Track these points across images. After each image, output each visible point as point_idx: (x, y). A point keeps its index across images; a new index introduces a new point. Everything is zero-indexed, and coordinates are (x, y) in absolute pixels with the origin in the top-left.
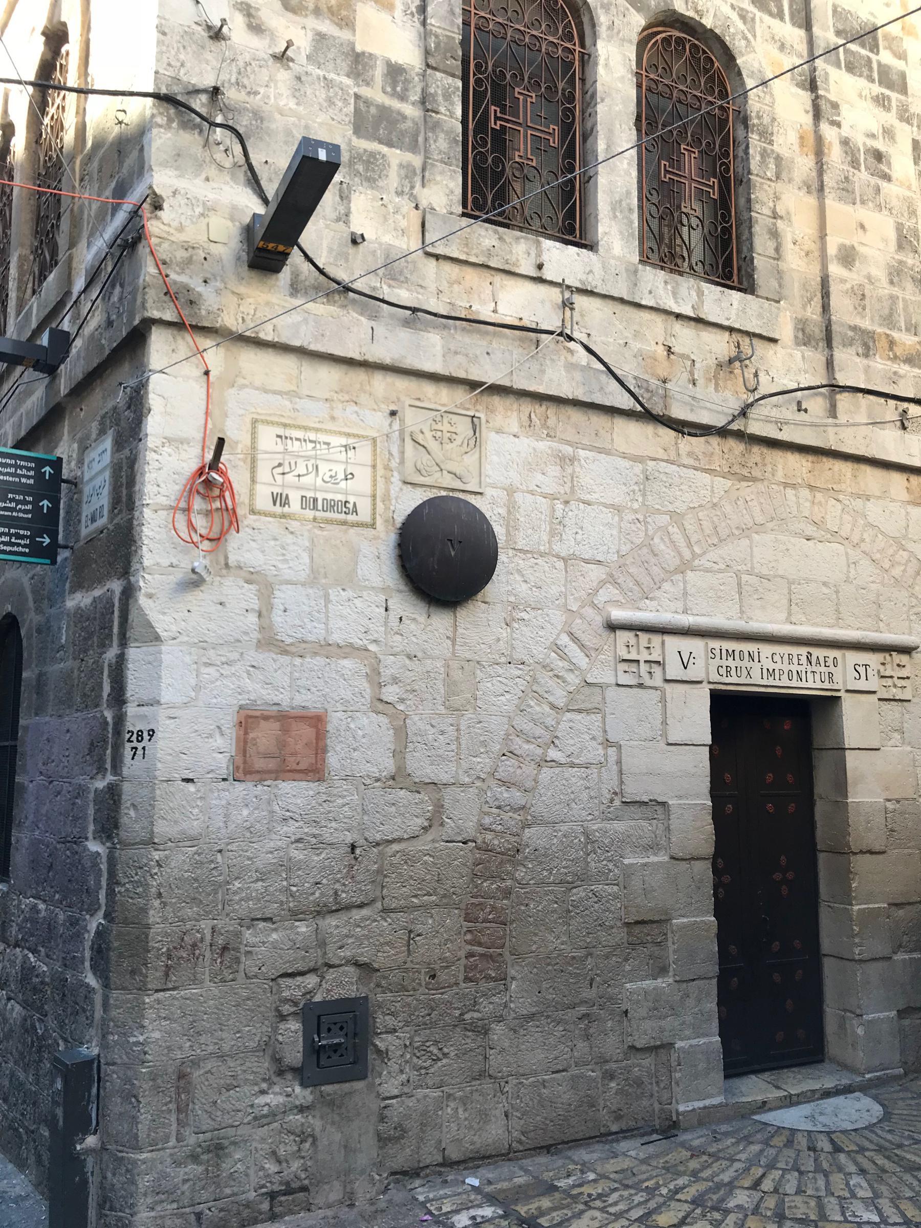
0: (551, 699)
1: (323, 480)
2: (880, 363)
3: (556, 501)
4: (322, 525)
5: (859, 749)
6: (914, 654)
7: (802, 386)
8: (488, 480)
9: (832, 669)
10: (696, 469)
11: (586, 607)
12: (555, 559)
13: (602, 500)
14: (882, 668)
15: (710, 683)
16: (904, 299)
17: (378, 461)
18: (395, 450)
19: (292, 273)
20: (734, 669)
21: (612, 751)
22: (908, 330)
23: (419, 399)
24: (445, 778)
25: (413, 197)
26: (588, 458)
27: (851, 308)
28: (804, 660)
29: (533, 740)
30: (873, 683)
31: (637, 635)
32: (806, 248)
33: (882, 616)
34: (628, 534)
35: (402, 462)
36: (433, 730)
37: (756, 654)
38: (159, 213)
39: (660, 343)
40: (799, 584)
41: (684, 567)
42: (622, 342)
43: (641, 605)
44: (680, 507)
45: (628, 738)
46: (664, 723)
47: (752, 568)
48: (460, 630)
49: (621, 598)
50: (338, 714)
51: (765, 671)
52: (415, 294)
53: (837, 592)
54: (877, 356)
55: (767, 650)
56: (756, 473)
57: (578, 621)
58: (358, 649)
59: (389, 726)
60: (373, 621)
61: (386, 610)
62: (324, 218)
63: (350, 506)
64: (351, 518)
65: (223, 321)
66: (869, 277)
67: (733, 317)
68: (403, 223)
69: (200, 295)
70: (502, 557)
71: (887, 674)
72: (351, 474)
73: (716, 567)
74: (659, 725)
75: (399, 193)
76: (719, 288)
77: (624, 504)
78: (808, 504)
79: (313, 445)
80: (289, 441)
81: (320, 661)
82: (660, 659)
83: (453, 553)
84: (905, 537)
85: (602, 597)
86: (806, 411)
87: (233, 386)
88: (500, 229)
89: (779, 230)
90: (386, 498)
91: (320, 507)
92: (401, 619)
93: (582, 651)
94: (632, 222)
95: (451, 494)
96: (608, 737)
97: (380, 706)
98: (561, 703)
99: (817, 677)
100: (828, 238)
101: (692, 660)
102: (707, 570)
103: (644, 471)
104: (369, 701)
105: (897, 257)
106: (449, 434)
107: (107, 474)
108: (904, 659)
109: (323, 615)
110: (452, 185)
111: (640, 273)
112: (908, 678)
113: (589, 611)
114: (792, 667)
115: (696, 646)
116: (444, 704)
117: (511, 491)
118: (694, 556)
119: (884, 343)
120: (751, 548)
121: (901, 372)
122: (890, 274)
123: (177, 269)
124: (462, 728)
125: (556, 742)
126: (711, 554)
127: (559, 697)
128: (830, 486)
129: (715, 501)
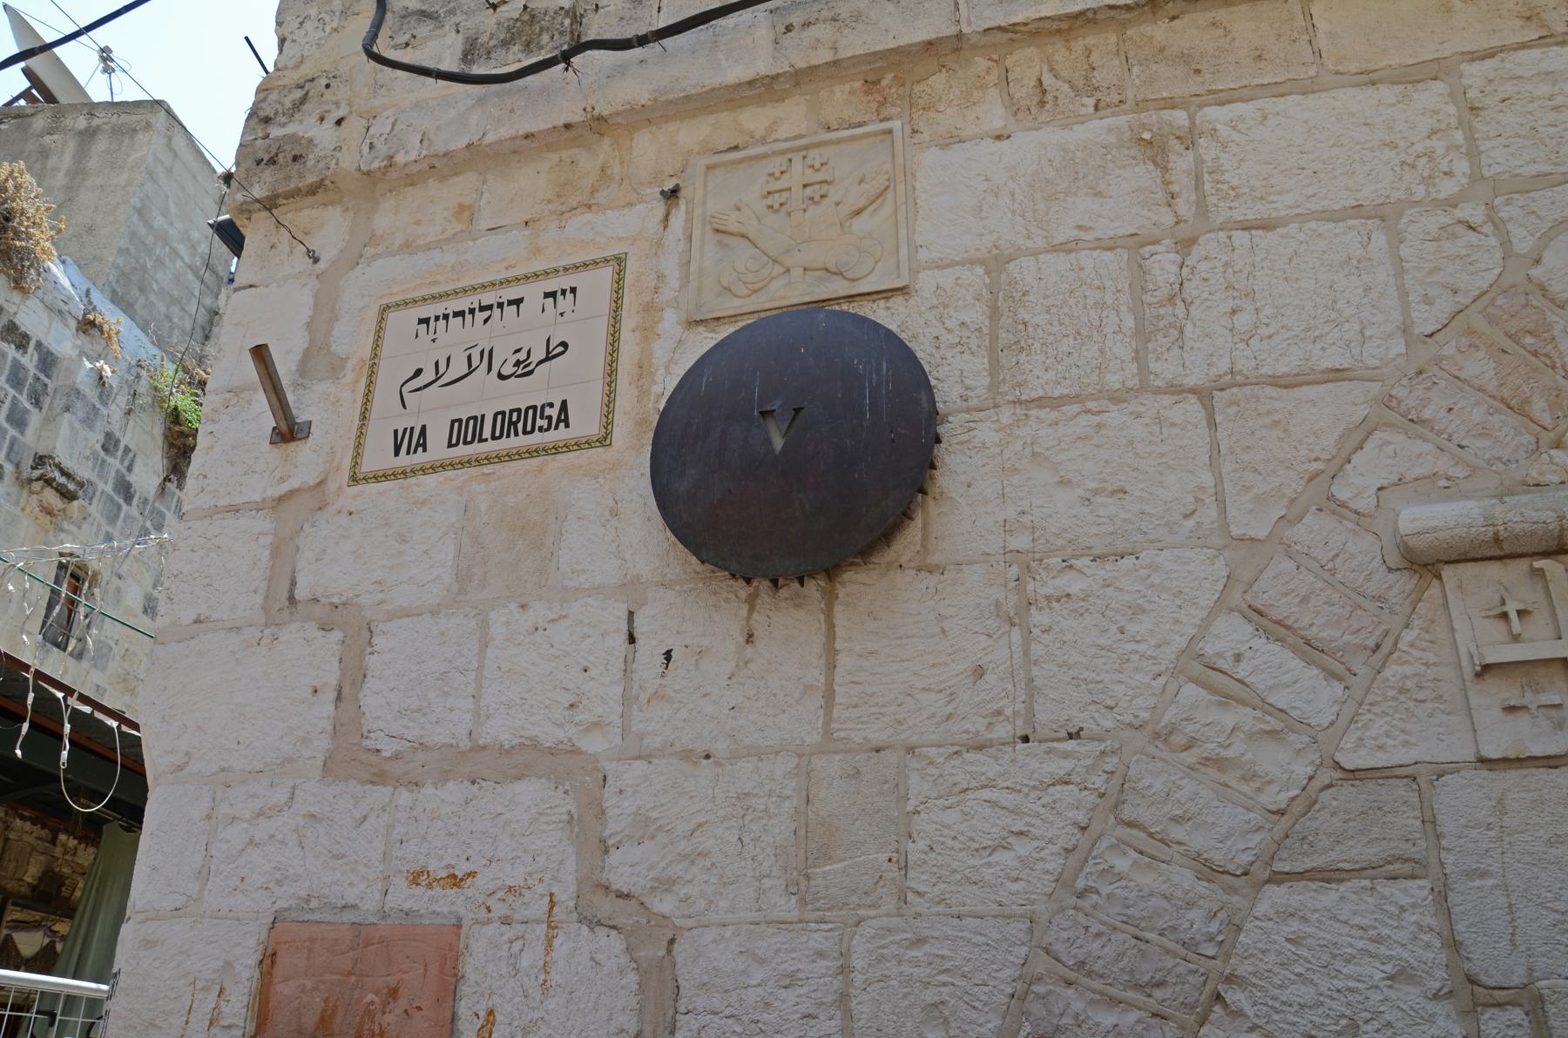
0: (1199, 841)
1: (501, 377)
3: (1148, 249)
4: (486, 470)
8: (923, 255)
12: (1166, 400)
13: (1313, 205)
18: (670, 266)
23: (736, 148)
26: (1241, 119)
29: (1130, 994)
34: (1431, 272)
36: (758, 975)
48: (844, 661)
49: (1443, 465)
50: (490, 930)
58: (551, 752)
59: (625, 959)
60: (593, 672)
61: (632, 639)
64: (560, 435)
65: (337, 164)
72: (564, 345)
77: (1397, 195)
79: (487, 313)
80: (442, 323)
81: (454, 791)
83: (778, 443)
87: (358, 264)
90: (643, 371)
91: (487, 433)
92: (668, 655)
93: (1310, 662)
96: (1474, 968)
97: (605, 907)
98: (1240, 851)
104: (572, 889)
106: (809, 191)
109: (471, 676)
116: (791, 889)
117: (996, 262)
123: (284, 119)
124: (858, 963)
125: (1234, 996)
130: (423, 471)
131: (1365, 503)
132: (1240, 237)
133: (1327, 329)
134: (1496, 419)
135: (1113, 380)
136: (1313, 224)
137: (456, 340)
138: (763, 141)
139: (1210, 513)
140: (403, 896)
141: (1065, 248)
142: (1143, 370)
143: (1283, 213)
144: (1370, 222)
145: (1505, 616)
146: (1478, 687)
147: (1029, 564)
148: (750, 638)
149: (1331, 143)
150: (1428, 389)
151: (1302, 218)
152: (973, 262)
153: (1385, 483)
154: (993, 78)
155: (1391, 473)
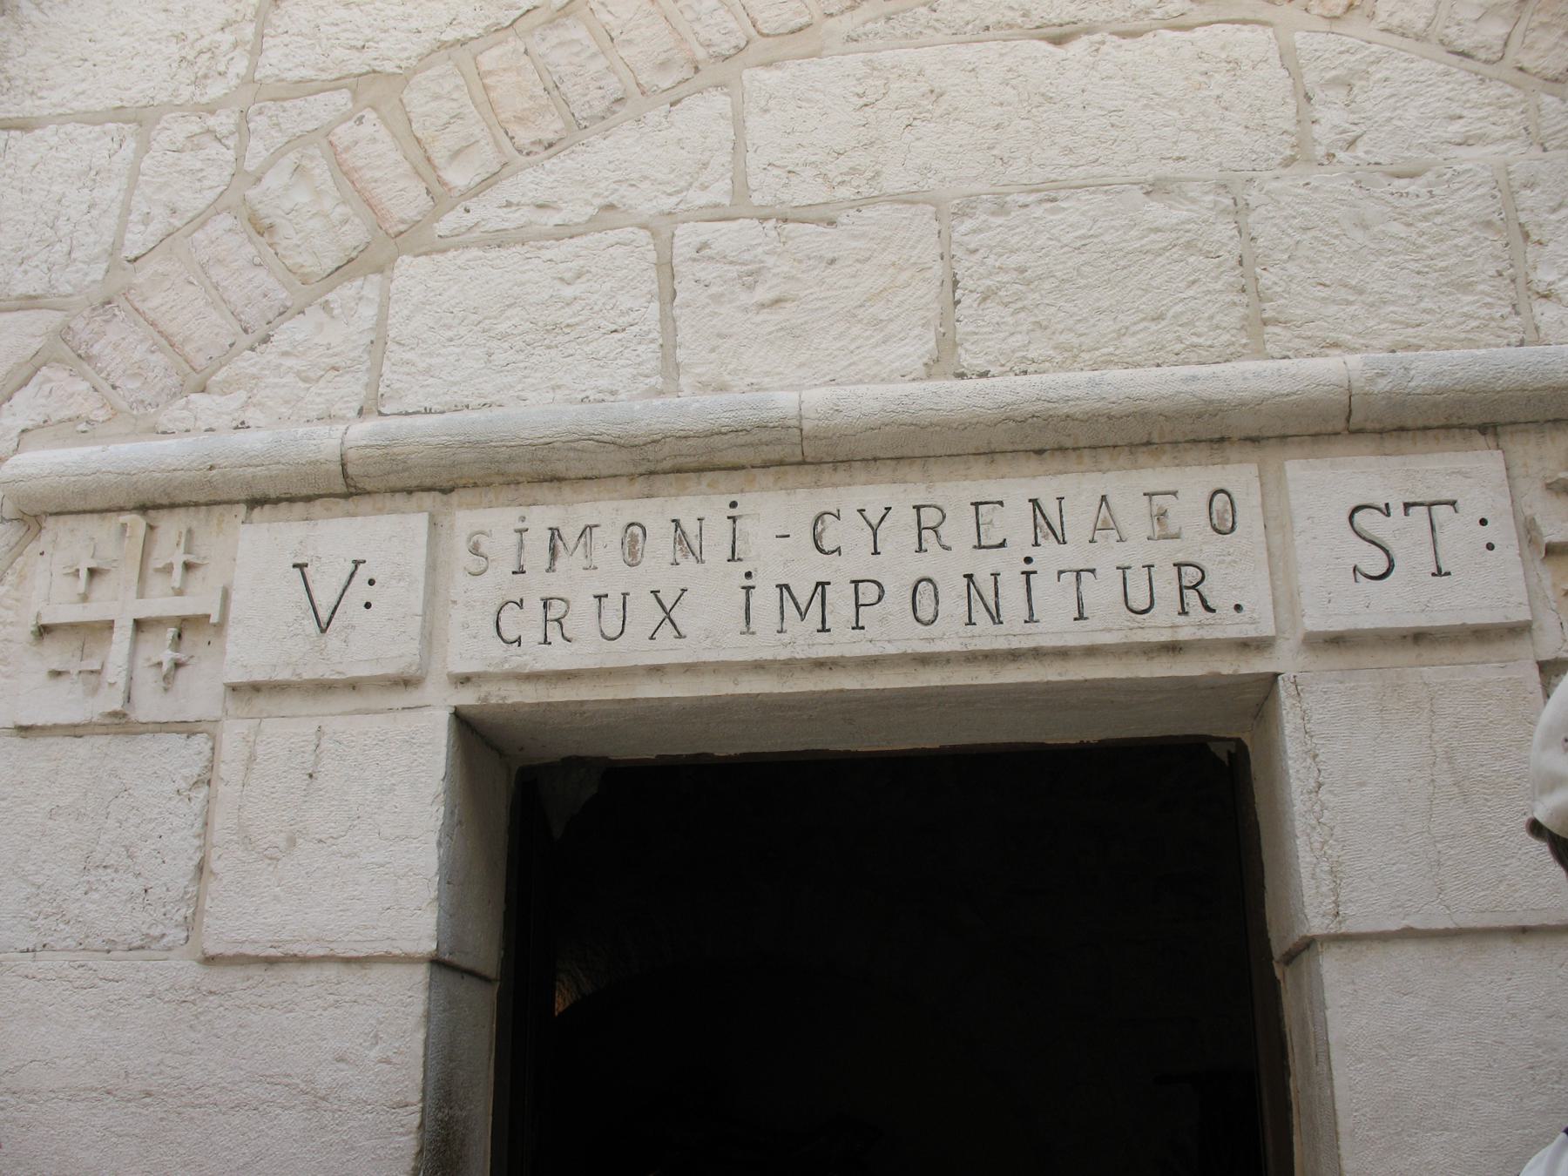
5: (1408, 934)
20: (584, 605)
28: (1013, 522)
33: (1544, 276)
40: (1001, 209)
43: (176, 413)
44: (394, 50)
45: (32, 940)
47: (741, 188)
51: (767, 598)
53: (1239, 209)
73: (552, 219)
74: (179, 872)
77: (163, 97)
99: (1102, 593)
101: (359, 590)
102: (499, 240)
118: (440, 197)
126: (527, 177)
133: (37, 249)
134: (153, 358)
136: (70, 127)
143: (45, 113)
144: (126, 127)
145: (77, 573)
146: (35, 649)
149: (121, 32)
150: (107, 321)
151: (62, 119)
153: (29, 424)
155: (39, 414)
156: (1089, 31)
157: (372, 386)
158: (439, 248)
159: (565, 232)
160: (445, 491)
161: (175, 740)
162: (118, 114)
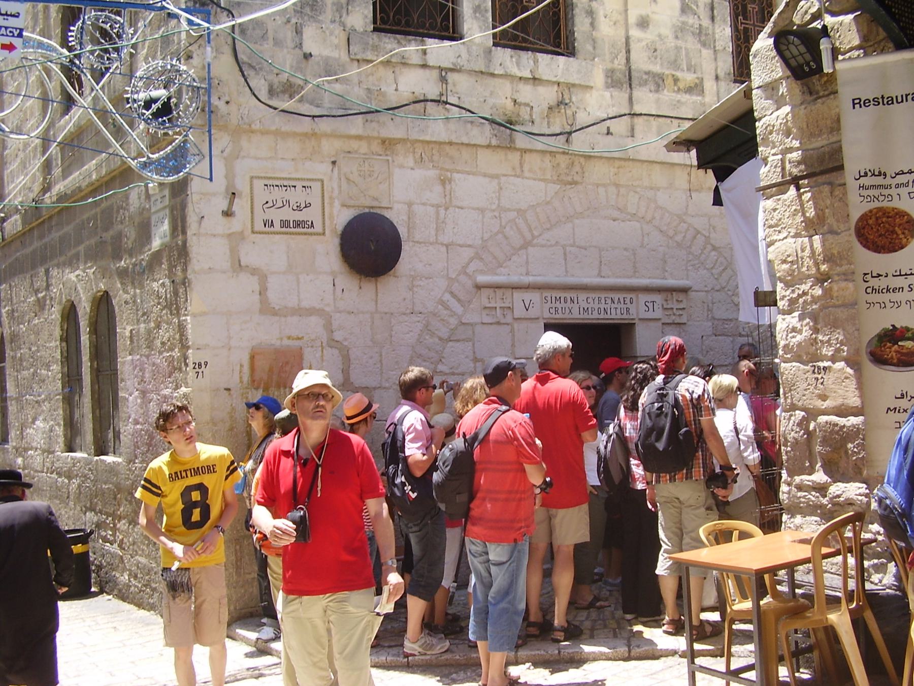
2: (668, 95)
6: (690, 293)
7: (610, 116)
9: (629, 305)
10: (535, 179)
11: (462, 276)
14: (665, 303)
15: (544, 318)
16: (686, 49)
17: (325, 194)
18: (335, 186)
19: (269, 85)
20: (560, 309)
21: (478, 364)
22: (688, 70)
23: (349, 152)
24: (374, 384)
25: (343, 25)
27: (646, 59)
28: (609, 301)
30: (658, 314)
31: (495, 292)
32: (614, 19)
33: (667, 268)
35: (340, 192)
36: (365, 357)
37: (576, 299)
38: (191, 61)
39: (509, 97)
41: (526, 245)
42: (482, 100)
46: (513, 345)
47: (574, 242)
48: (379, 294)
50: (309, 349)
51: (582, 309)
52: (345, 86)
53: (634, 254)
54: (665, 91)
55: (583, 296)
56: (577, 178)
57: (457, 284)
58: (318, 310)
62: (287, 47)
63: (310, 223)
66: (660, 36)
67: (560, 74)
68: (336, 41)
69: (217, 107)
70: (405, 247)
71: (669, 307)
73: (549, 243)
75: (333, 22)
76: (550, 56)
78: (614, 197)
80: (272, 187)
81: (295, 319)
82: (510, 305)
83: (373, 248)
84: (686, 214)
85: (471, 269)
86: (612, 134)
88: (398, 36)
89: (594, 9)
90: (331, 217)
91: (292, 226)
94: (487, 18)
95: (372, 211)
98: (445, 336)
99: (619, 311)
100: (629, 12)
101: (531, 305)
102: (542, 246)
103: (499, 184)
105: (680, 19)
107: (167, 211)
108: (681, 296)
110: (366, 12)
111: (493, 53)
112: (684, 309)
113: (463, 278)
114: (600, 306)
115: (534, 297)
117: (410, 205)
119: (669, 81)
120: (574, 229)
121: (683, 100)
122: (676, 32)
124: (383, 354)
125: (443, 360)
127: (444, 332)
128: (630, 183)
129: (548, 199)
130: (274, 233)
131: (471, 274)
132: (457, 210)
135: (431, 240)
137: (278, 195)
138: (356, 152)
139: (445, 272)
140: (286, 342)
141: (424, 204)
142: (437, 239)
147: (414, 278)
148: (360, 288)
152: (405, 203)
154: (411, 150)
156: (618, 220)
157: (527, 270)
158: (533, 246)
159: (551, 246)
160: (539, 289)
161: (506, 326)
162: (478, 209)
